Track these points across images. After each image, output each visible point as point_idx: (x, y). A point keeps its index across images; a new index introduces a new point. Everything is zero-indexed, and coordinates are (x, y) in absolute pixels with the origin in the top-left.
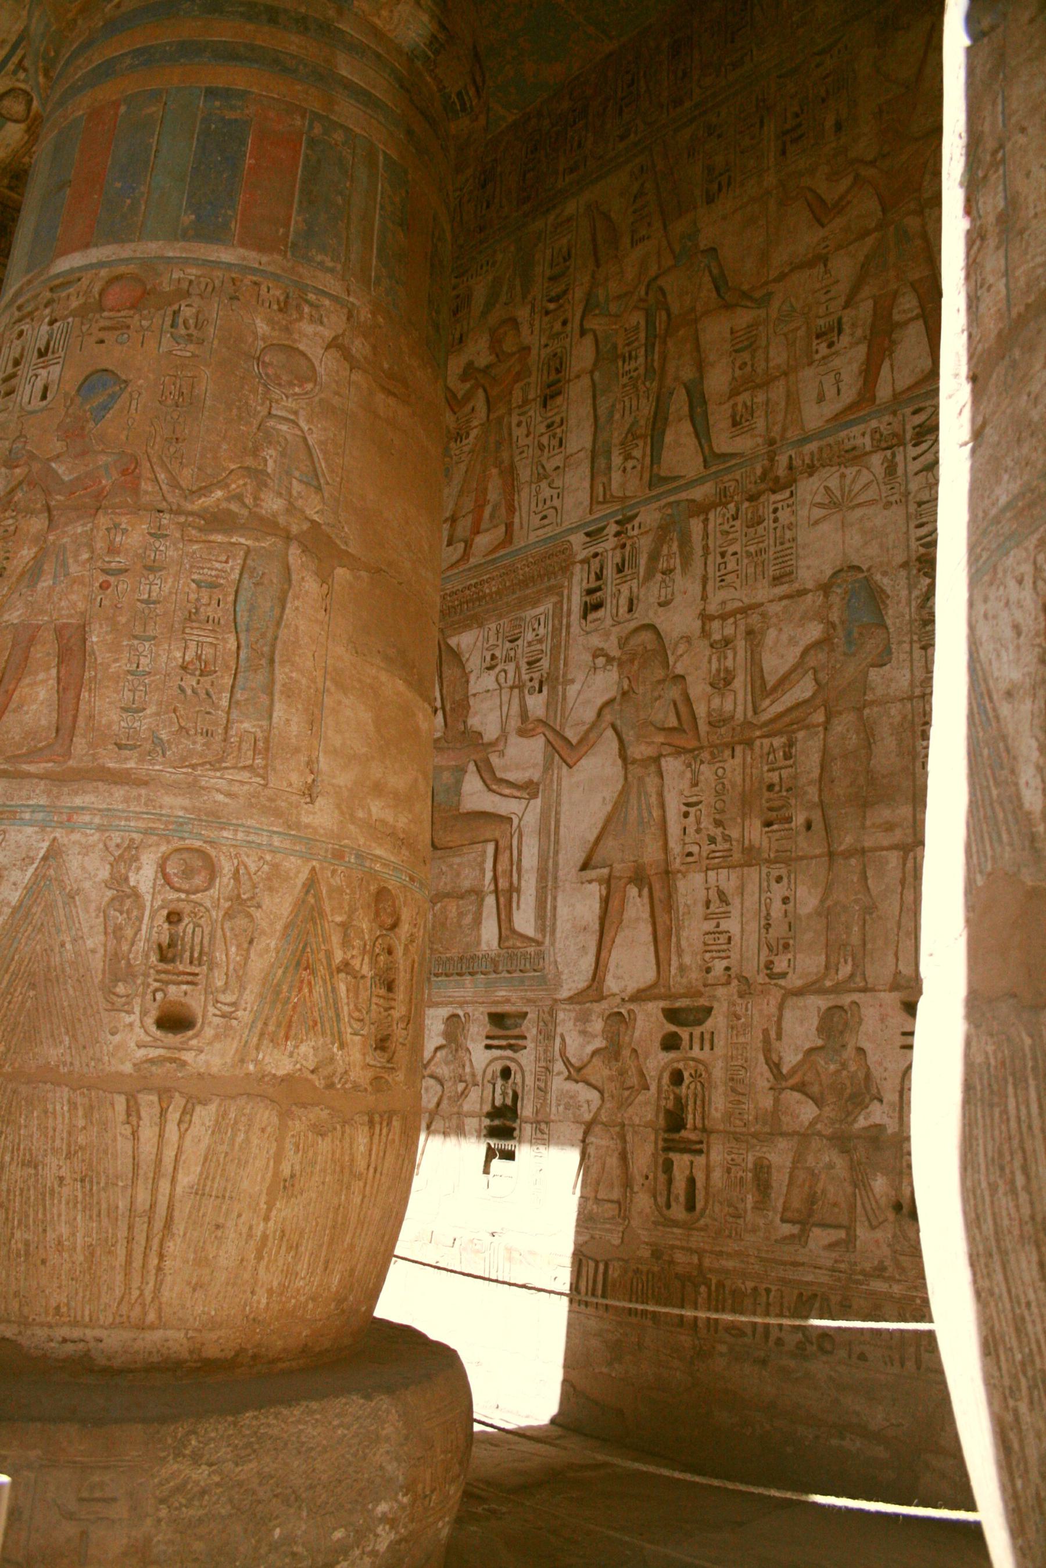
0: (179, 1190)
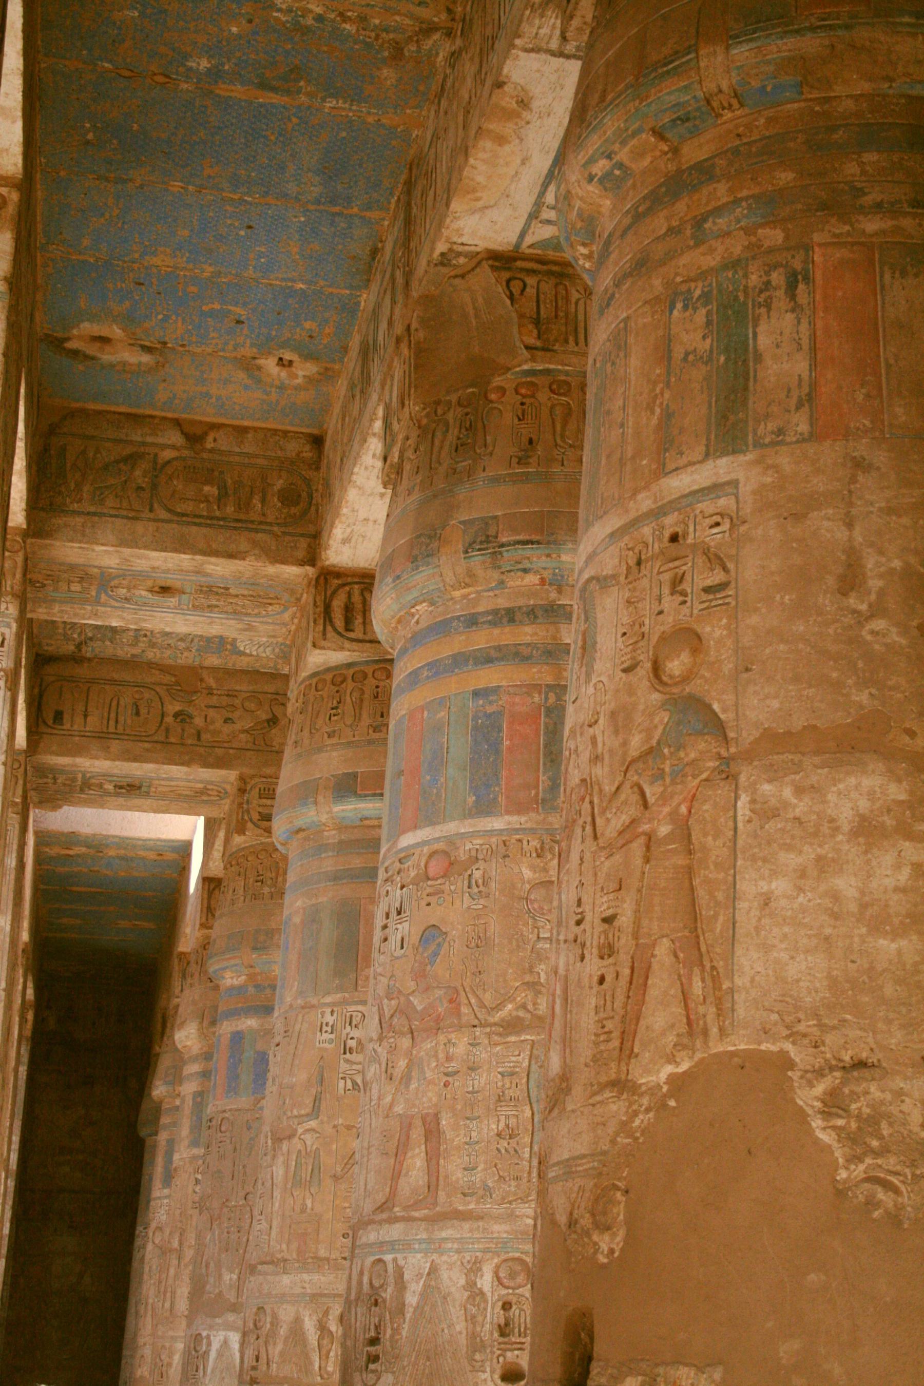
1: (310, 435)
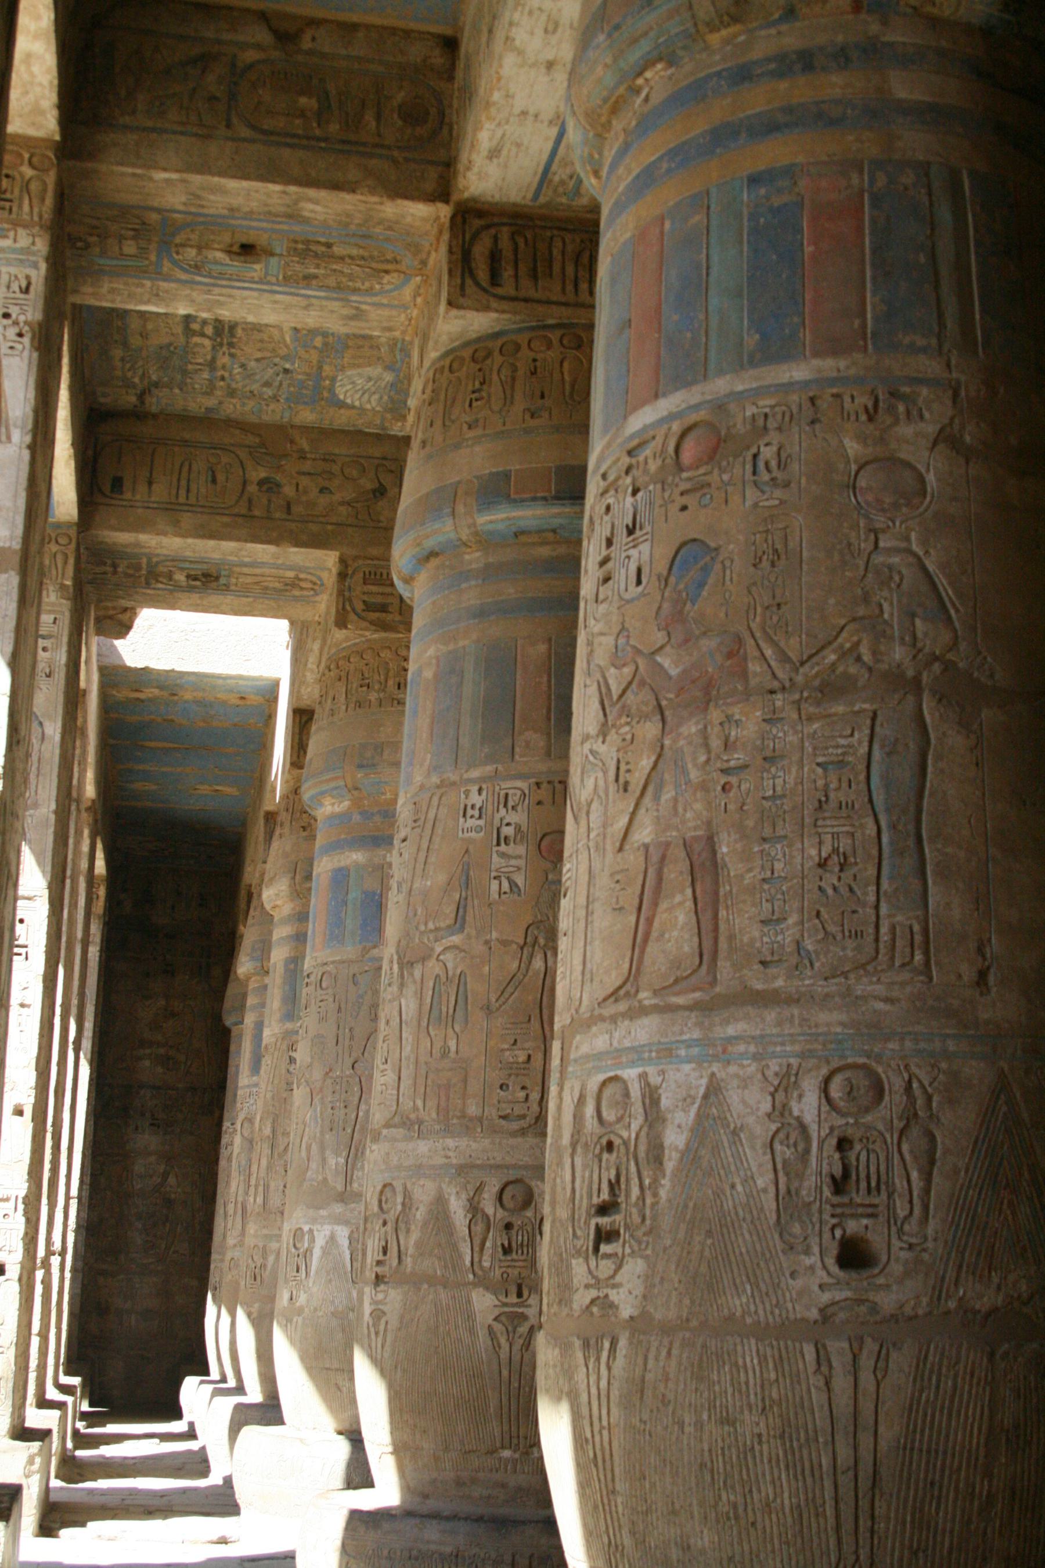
0: (883, 1445)
1: (439, 36)
